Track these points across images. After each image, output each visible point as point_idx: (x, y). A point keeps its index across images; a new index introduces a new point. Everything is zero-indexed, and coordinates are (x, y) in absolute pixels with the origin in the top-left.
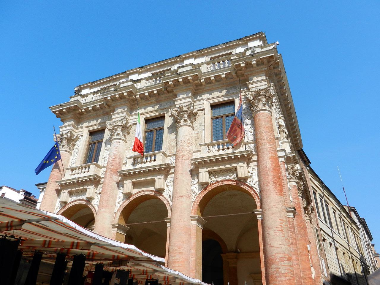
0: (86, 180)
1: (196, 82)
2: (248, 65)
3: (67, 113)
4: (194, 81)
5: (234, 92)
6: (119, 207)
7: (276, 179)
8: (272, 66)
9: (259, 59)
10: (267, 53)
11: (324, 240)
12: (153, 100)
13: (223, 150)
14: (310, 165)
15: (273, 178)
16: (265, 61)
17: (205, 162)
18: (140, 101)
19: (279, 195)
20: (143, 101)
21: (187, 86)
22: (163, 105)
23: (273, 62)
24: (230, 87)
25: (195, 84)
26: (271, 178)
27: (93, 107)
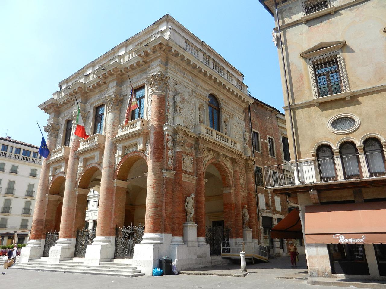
0: (60, 159)
1: (118, 73)
2: (147, 54)
3: (49, 109)
4: (116, 72)
7: (156, 149)
8: (166, 51)
9: (153, 48)
10: (156, 41)
12: (97, 90)
15: (154, 149)
16: (157, 48)
18: (90, 93)
19: (156, 161)
20: (92, 92)
21: (113, 77)
23: (164, 47)
24: (143, 73)
25: (119, 74)
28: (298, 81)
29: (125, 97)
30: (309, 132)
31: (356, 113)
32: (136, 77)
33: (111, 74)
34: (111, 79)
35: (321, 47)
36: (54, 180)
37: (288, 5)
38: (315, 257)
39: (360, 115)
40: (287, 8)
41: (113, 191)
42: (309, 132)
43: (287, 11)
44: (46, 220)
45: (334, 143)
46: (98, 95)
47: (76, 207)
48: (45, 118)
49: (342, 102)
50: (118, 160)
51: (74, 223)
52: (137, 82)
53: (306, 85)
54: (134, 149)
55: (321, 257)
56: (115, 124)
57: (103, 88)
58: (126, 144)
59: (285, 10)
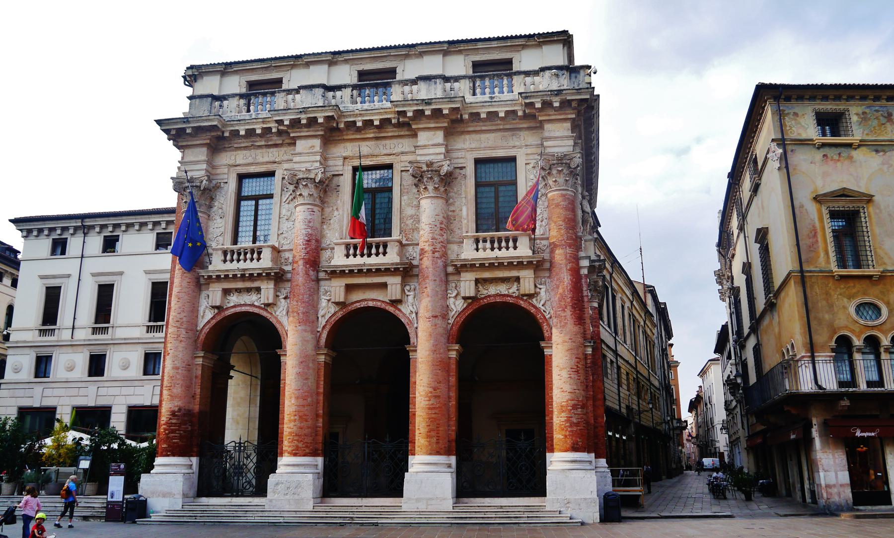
5: (517, 144)
6: (324, 323)
11: (605, 356)
13: (500, 248)
14: (599, 229)
17: (473, 266)
22: (388, 147)
26: (569, 300)
27: (247, 130)
28: (811, 235)
29: (458, 171)
30: (827, 316)
31: (883, 300)
32: (491, 136)
33: (437, 113)
34: (432, 125)
35: (843, 194)
36: (219, 318)
37: (793, 108)
38: (834, 486)
39: (888, 304)
40: (792, 111)
41: (448, 364)
42: (827, 316)
43: (791, 116)
44: (201, 412)
45: (858, 337)
46: (368, 143)
47: (321, 390)
48: (168, 158)
49: (867, 282)
50: (457, 306)
51: (321, 425)
52: (494, 148)
53: (821, 244)
54: (503, 289)
55: (841, 485)
56: (443, 226)
57: (390, 134)
58: (487, 275)
59: (788, 114)
